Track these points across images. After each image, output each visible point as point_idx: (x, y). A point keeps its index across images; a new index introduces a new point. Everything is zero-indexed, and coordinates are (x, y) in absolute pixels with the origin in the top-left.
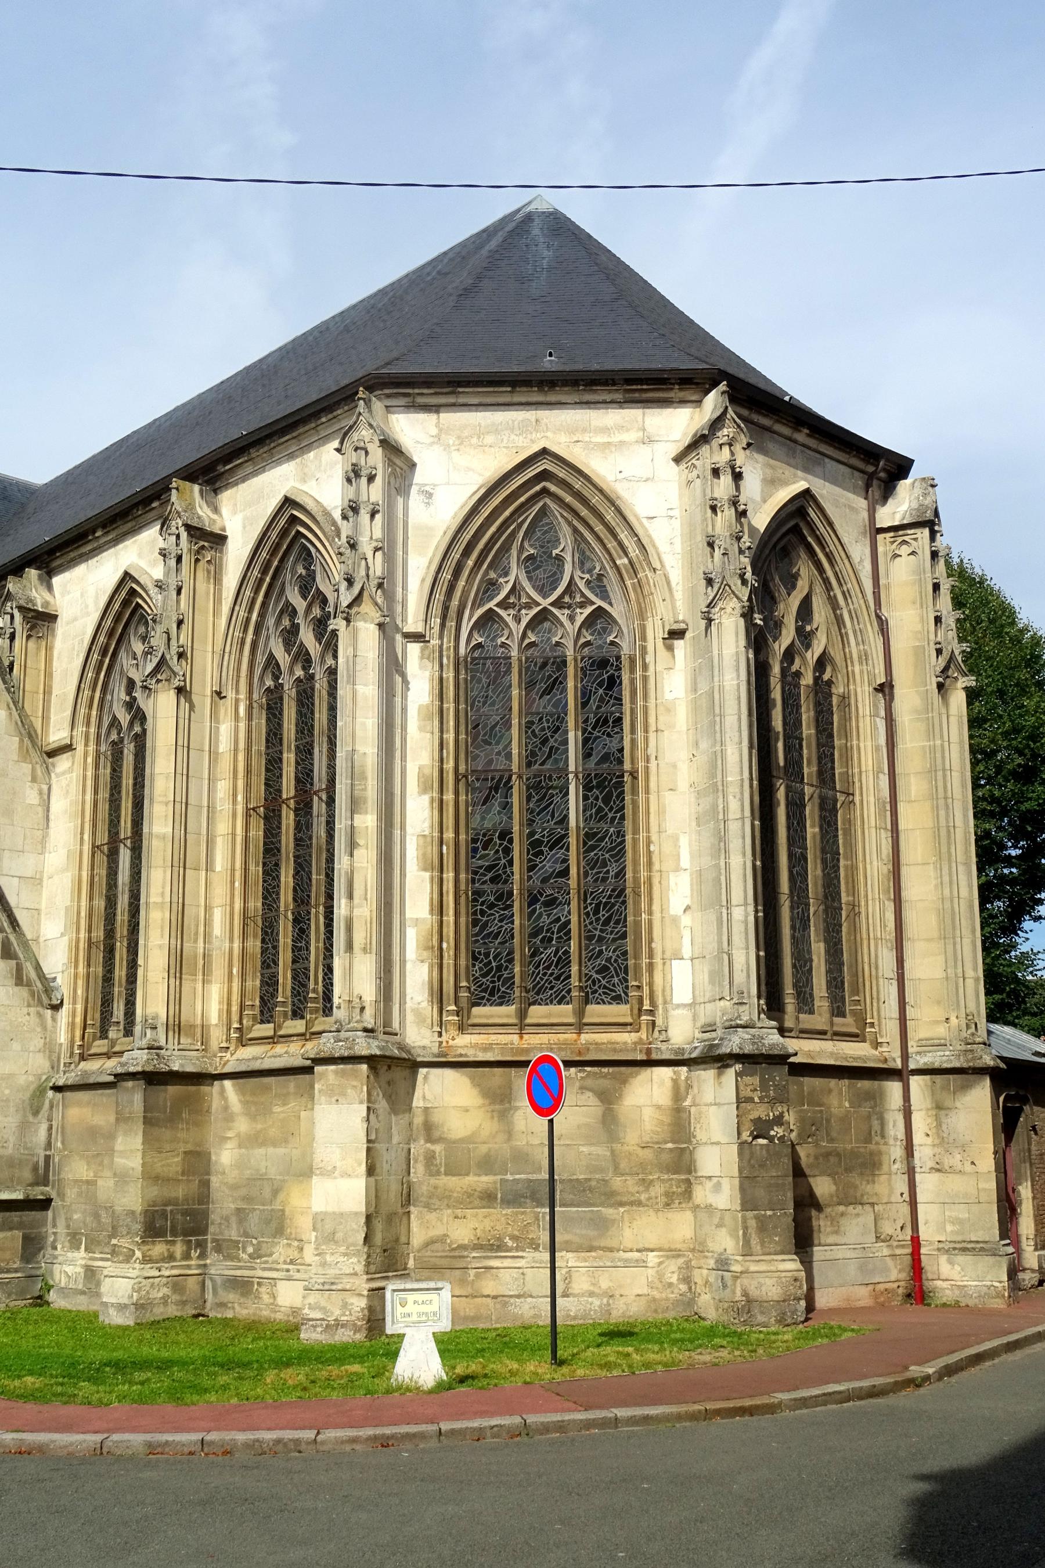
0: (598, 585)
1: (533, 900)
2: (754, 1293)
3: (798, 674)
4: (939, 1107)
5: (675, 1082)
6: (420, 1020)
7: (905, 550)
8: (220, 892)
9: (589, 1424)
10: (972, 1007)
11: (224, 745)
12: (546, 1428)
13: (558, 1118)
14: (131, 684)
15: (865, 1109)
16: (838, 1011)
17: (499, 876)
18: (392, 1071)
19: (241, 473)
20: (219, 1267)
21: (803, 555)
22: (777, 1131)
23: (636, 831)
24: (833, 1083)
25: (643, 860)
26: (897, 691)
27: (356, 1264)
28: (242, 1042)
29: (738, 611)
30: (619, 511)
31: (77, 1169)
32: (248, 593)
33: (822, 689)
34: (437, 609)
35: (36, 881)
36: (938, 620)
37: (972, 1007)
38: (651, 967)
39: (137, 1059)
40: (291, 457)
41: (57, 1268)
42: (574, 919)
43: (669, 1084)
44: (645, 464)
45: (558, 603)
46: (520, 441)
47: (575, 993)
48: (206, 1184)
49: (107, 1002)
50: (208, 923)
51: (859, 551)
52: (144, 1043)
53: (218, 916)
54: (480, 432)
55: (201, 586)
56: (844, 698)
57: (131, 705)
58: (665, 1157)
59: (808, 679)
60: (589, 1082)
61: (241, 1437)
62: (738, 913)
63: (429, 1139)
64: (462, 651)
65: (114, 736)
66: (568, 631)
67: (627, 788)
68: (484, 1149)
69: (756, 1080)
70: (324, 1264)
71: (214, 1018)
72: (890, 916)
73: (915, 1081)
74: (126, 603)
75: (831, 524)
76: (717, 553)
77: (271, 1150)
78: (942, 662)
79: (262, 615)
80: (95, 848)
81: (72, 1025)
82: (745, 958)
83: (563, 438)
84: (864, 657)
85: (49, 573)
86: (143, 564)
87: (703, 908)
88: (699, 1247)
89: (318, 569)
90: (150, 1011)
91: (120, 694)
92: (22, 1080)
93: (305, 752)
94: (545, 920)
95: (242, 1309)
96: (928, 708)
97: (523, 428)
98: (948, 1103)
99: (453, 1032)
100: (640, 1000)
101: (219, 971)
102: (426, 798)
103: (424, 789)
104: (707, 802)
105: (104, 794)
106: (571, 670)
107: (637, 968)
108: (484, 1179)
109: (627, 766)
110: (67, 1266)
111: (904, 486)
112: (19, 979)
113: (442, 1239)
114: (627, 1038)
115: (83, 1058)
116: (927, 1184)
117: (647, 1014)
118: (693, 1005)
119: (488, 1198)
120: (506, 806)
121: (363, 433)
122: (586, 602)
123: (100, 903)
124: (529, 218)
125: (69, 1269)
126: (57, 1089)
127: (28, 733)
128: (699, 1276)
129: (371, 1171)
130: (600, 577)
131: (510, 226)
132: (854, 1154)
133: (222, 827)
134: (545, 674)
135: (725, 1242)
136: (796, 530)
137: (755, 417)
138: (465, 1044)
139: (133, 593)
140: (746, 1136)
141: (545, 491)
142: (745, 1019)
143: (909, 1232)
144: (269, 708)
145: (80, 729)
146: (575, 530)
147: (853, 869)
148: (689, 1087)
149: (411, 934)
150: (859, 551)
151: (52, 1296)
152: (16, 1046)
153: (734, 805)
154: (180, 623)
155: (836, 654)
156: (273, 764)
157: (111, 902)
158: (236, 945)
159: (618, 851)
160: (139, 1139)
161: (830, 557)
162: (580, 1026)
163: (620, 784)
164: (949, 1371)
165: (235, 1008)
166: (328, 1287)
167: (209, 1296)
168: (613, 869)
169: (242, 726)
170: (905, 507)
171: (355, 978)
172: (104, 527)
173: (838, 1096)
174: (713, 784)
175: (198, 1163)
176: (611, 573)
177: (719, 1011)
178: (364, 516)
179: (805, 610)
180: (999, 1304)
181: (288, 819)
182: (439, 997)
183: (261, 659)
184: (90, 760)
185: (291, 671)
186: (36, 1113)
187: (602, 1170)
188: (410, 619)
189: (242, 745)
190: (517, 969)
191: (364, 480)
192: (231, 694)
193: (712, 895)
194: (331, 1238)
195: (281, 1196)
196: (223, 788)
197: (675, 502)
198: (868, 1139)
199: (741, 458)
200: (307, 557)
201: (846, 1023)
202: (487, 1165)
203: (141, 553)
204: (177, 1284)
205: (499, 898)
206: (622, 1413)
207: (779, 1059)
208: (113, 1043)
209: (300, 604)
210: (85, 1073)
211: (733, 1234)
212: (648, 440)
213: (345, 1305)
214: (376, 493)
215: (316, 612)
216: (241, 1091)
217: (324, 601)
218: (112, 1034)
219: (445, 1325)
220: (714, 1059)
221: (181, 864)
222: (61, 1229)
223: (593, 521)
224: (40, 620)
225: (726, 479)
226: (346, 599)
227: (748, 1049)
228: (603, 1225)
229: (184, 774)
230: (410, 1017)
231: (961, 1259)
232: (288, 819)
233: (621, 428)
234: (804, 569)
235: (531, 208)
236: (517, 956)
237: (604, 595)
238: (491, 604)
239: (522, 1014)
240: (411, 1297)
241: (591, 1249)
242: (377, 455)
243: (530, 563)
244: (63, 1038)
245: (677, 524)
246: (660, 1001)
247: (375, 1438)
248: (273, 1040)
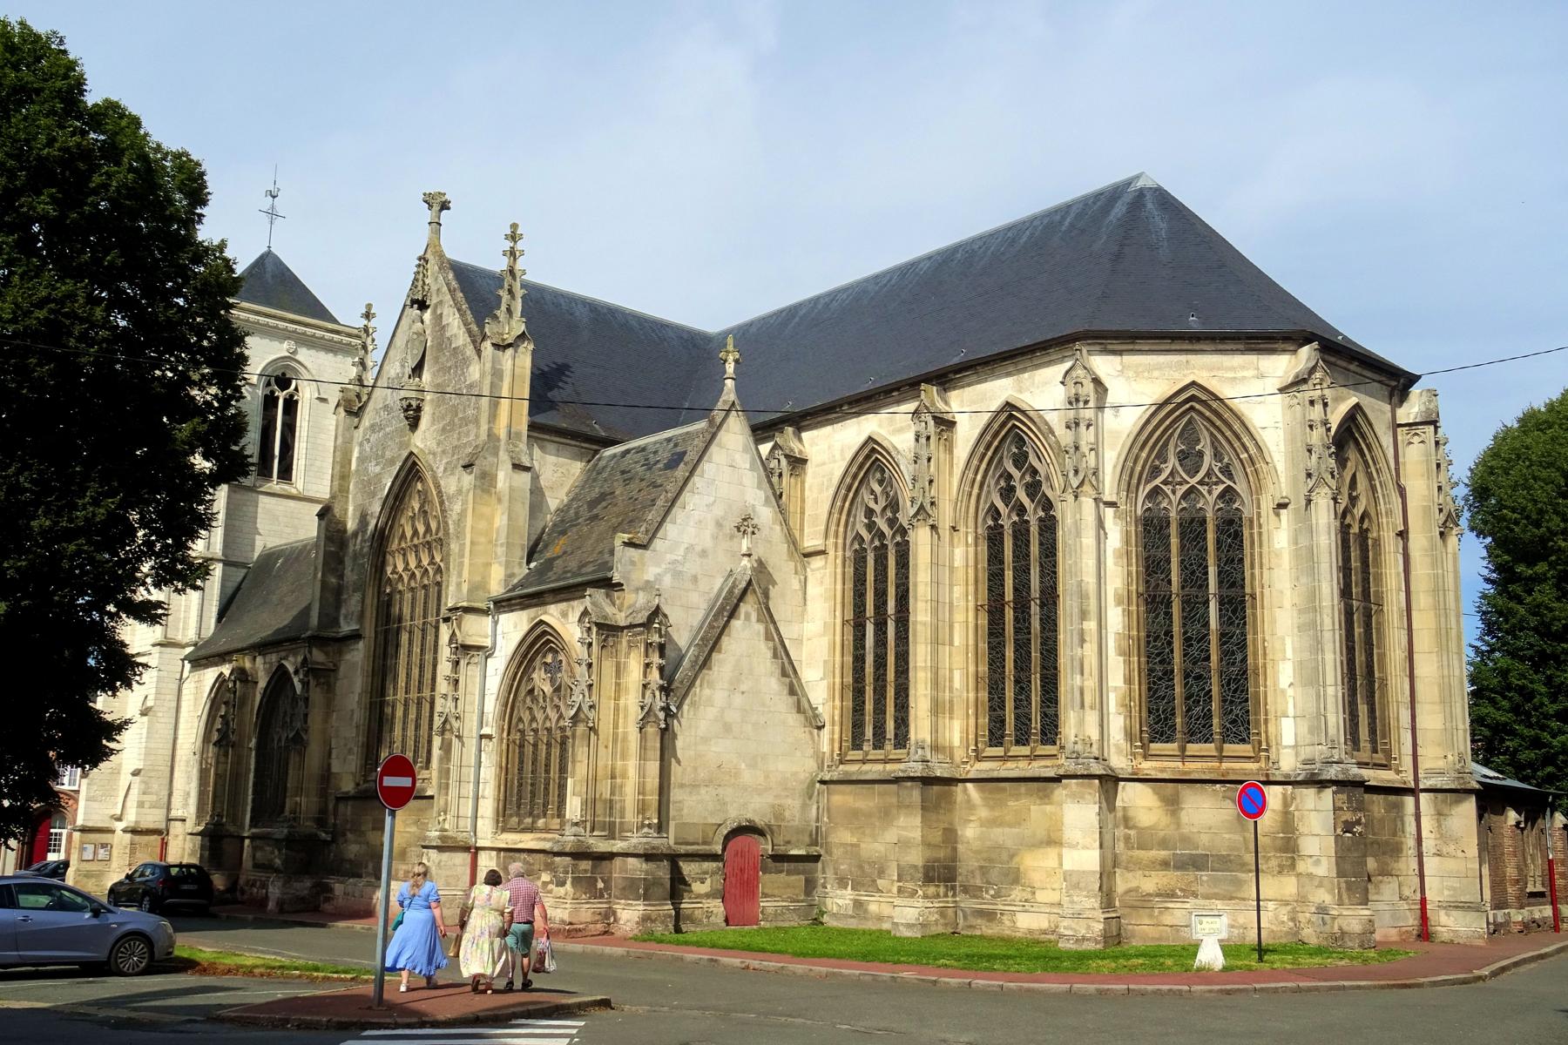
0: (1227, 471)
1: (1187, 676)
2: (1345, 928)
3: (1349, 526)
4: (1440, 814)
5: (1284, 795)
6: (1119, 751)
7: (1416, 439)
8: (959, 660)
9: (1331, 988)
10: (1462, 748)
11: (959, 561)
12: (1309, 990)
13: (1259, 820)
14: (870, 513)
16: (1375, 751)
17: (1166, 661)
18: (1110, 782)
19: (967, 380)
20: (968, 903)
21: (1352, 445)
22: (1358, 829)
23: (1255, 633)
24: (1375, 797)
26: (1411, 536)
27: (1094, 902)
28: (979, 759)
29: (1330, 495)
30: (1243, 424)
31: (843, 836)
32: (975, 462)
33: (1364, 534)
34: (1124, 486)
35: (799, 641)
36: (1440, 488)
37: (1462, 748)
38: (1266, 721)
39: (917, 769)
40: (1009, 374)
41: (829, 901)
42: (1215, 690)
44: (1262, 392)
45: (1201, 483)
46: (1177, 375)
47: (1216, 737)
48: (955, 849)
49: (858, 726)
50: (951, 680)
51: (1387, 441)
52: (917, 757)
53: (957, 675)
54: (1150, 369)
55: (942, 456)
56: (1377, 541)
57: (871, 526)
58: (1279, 843)
59: (1355, 529)
60: (1229, 794)
61: (1150, 988)
62: (1331, 691)
63: (1127, 827)
64: (1139, 512)
65: (857, 546)
66: (1209, 503)
67: (1248, 605)
68: (1162, 834)
69: (1344, 797)
70: (1072, 902)
71: (956, 742)
72: (1407, 687)
73: (1422, 796)
74: (867, 457)
75: (1371, 425)
76: (1314, 457)
77: (1007, 830)
78: (1442, 517)
79: (984, 477)
81: (832, 740)
82: (1335, 719)
83: (1205, 374)
84: (1389, 513)
85: (799, 429)
86: (883, 432)
87: (1304, 685)
88: (1302, 899)
89: (1030, 451)
90: (920, 737)
91: (861, 518)
92: (802, 776)
93: (1022, 572)
94: (1195, 689)
95: (989, 930)
96: (1433, 547)
97: (1179, 366)
98: (1446, 811)
99: (1140, 759)
100: (1260, 743)
101: (959, 711)
102: (1120, 609)
103: (1119, 603)
104: (1307, 618)
105: (850, 585)
106: (1210, 528)
107: (1257, 722)
109: (1248, 590)
110: (838, 900)
111: (1415, 391)
112: (799, 710)
113: (1136, 889)
114: (1252, 766)
115: (841, 762)
116: (1431, 864)
117: (1262, 750)
118: (1296, 746)
119: (1165, 865)
120: (1169, 615)
121: (1080, 372)
123: (849, 659)
124: (1141, 193)
125: (840, 902)
126: (823, 782)
127: (792, 542)
128: (1301, 917)
129: (1101, 846)
130: (1228, 465)
131: (1127, 198)
132: (1387, 843)
133: (959, 617)
134: (1193, 528)
135: (1324, 896)
136: (1349, 430)
137: (1332, 359)
138: (1149, 767)
139: (873, 450)
140: (1339, 831)
141: (1192, 408)
142: (1336, 758)
143: (1418, 896)
144: (989, 538)
145: (831, 540)
146: (1212, 434)
147: (1382, 656)
148: (1293, 798)
149: (1112, 696)
150: (1387, 441)
151: (825, 918)
152: (798, 754)
153: (1327, 621)
154: (931, 482)
155: (1373, 513)
156: (996, 578)
158: (972, 695)
159: (1243, 646)
160: (918, 821)
161: (1369, 447)
162: (1221, 758)
163: (1244, 601)
164: (1494, 974)
165: (972, 736)
166: (1077, 916)
167: (961, 921)
168: (1239, 657)
169: (971, 550)
170: (1416, 409)
171: (1076, 725)
172: (850, 403)
173: (1378, 804)
174: (1311, 605)
175: (950, 836)
176: (1236, 463)
177: (1320, 752)
178: (1083, 427)
180: (1480, 943)
181: (1009, 614)
182: (1129, 736)
183: (984, 507)
184: (839, 561)
185: (1009, 517)
186: (810, 798)
187: (1238, 849)
188: (1107, 491)
189: (971, 562)
190: (1178, 720)
191: (1081, 405)
192: (962, 529)
193: (1310, 677)
194: (1077, 886)
195: (1016, 859)
196: (958, 591)
197: (1280, 418)
198: (1395, 834)
199: (1327, 392)
200: (1020, 442)
201: (1379, 758)
202: (1164, 844)
203: (894, 427)
204: (942, 912)
205: (1165, 673)
206: (1346, 983)
207: (1359, 784)
208: (867, 754)
209: (1016, 474)
210: (846, 773)
211: (1331, 892)
212: (1261, 376)
213: (1089, 927)
214: (1088, 414)
215: (1028, 478)
216: (981, 790)
217: (1035, 472)
219: (1224, 935)
220: (1315, 782)
221: (936, 642)
222: (830, 874)
223: (1224, 429)
224: (797, 463)
225: (1319, 407)
226: (1075, 482)
227: (1341, 777)
229: (936, 583)
230: (1113, 749)
231: (1454, 913)
232: (1009, 614)
233: (1243, 368)
234: (1352, 454)
235: (1140, 184)
236: (1178, 712)
237: (1230, 477)
238: (1157, 482)
239: (1183, 749)
240: (1205, 919)
242: (1089, 388)
243: (1183, 457)
244: (826, 748)
245: (1281, 432)
246: (1273, 743)
247: (1221, 991)
248: (1005, 758)
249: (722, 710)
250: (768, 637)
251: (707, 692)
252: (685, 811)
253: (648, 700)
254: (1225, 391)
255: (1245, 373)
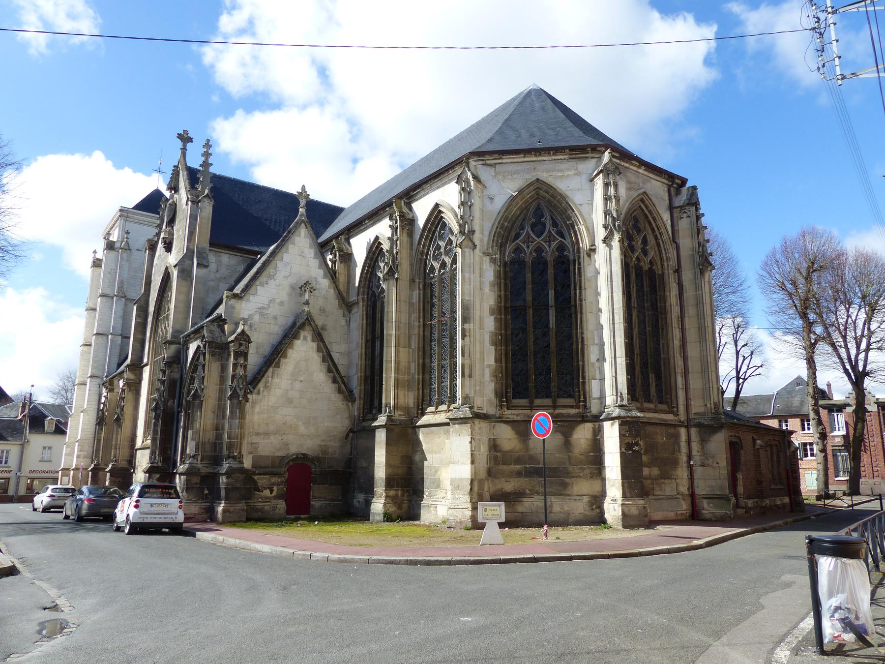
5: (594, 429)
15: (672, 441)
19: (419, 195)
22: (636, 448)
25: (579, 340)
27: (467, 498)
43: (591, 430)
66: (550, 251)
80: (367, 341)
108: (518, 467)
109: (573, 303)
114: (573, 411)
116: (698, 472)
119: (519, 474)
122: (556, 239)
123: (369, 362)
129: (472, 462)
145: (361, 296)
150: (666, 217)
157: (373, 362)
159: (570, 337)
169: (422, 292)
179: (645, 242)
195: (439, 473)
198: (674, 453)
202: (518, 461)
212: (579, 174)
213: (463, 513)
218: (374, 412)
228: (565, 485)
233: (568, 169)
237: (562, 236)
241: (560, 495)
249: (287, 391)
250: (319, 350)
251: (276, 380)
252: (260, 449)
253: (234, 385)
254: (550, 180)
255: (569, 173)
